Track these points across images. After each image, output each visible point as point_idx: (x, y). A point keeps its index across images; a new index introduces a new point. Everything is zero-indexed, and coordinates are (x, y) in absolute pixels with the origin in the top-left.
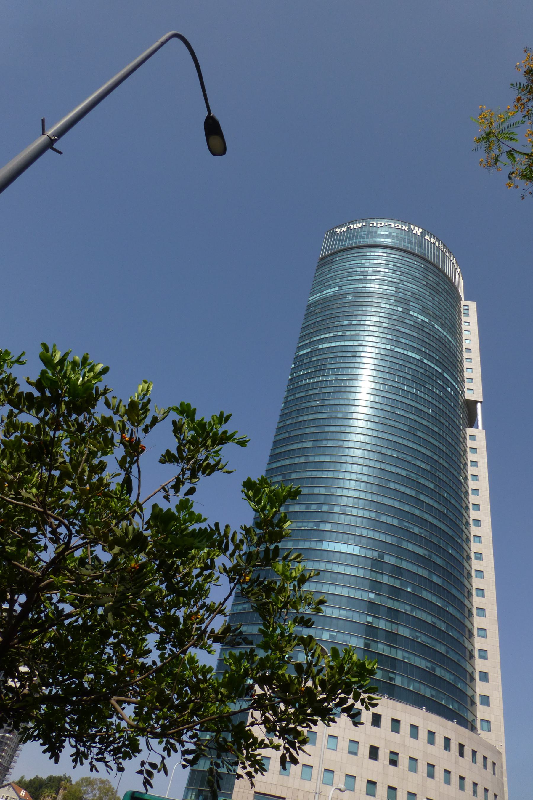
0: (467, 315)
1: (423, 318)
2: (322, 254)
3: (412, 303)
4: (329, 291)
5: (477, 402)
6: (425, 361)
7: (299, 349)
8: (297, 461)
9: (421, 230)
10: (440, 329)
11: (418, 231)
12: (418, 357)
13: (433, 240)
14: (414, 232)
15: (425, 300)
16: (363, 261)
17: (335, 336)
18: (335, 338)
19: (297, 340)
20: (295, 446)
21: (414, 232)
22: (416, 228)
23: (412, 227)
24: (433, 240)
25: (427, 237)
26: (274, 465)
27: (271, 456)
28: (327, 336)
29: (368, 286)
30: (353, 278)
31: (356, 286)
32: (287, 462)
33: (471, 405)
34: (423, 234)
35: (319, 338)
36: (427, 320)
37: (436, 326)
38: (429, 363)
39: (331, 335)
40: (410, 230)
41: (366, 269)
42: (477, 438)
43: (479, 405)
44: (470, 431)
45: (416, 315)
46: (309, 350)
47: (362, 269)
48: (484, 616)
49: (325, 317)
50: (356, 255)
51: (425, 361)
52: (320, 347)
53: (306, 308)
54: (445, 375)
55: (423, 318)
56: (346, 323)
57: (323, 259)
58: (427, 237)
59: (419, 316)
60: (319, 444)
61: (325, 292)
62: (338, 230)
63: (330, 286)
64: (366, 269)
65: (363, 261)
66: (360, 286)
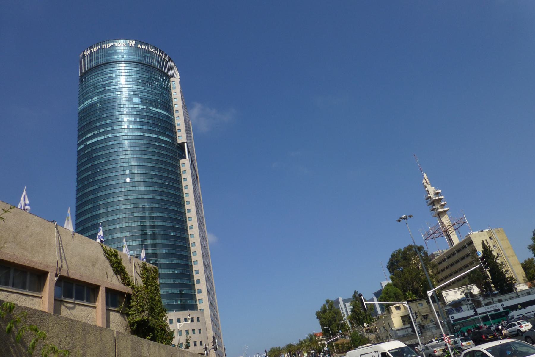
0: (174, 87)
1: (142, 107)
2: (81, 72)
3: (134, 99)
4: (87, 102)
5: (184, 143)
6: (146, 135)
7: (79, 145)
8: (88, 216)
9: (134, 42)
10: (154, 109)
11: (132, 43)
12: (142, 134)
13: (143, 47)
14: (130, 45)
15: (142, 94)
16: (102, 77)
17: (94, 134)
18: (95, 136)
19: (77, 139)
20: (86, 208)
21: (130, 45)
22: (131, 41)
23: (128, 41)
24: (143, 47)
25: (139, 46)
26: (80, 220)
27: (77, 215)
28: (90, 135)
29: (107, 94)
30: (98, 91)
31: (101, 96)
32: (83, 218)
33: (182, 145)
34: (136, 45)
35: (86, 137)
36: (145, 107)
37: (151, 108)
38: (149, 135)
39: (92, 134)
40: (128, 45)
41: (105, 83)
42: (185, 164)
43: (186, 144)
44: (182, 161)
45: (137, 106)
46: (83, 146)
47: (103, 83)
48: (196, 255)
49: (88, 122)
50: (99, 72)
51: (146, 135)
52: (88, 143)
53: (77, 115)
54: (160, 137)
55: (142, 107)
56: (98, 124)
57: (82, 76)
58: (139, 46)
59: (140, 106)
60: (96, 204)
61: (85, 103)
62: (85, 53)
63: (87, 99)
64: (105, 83)
65: (102, 77)
66: (103, 96)
